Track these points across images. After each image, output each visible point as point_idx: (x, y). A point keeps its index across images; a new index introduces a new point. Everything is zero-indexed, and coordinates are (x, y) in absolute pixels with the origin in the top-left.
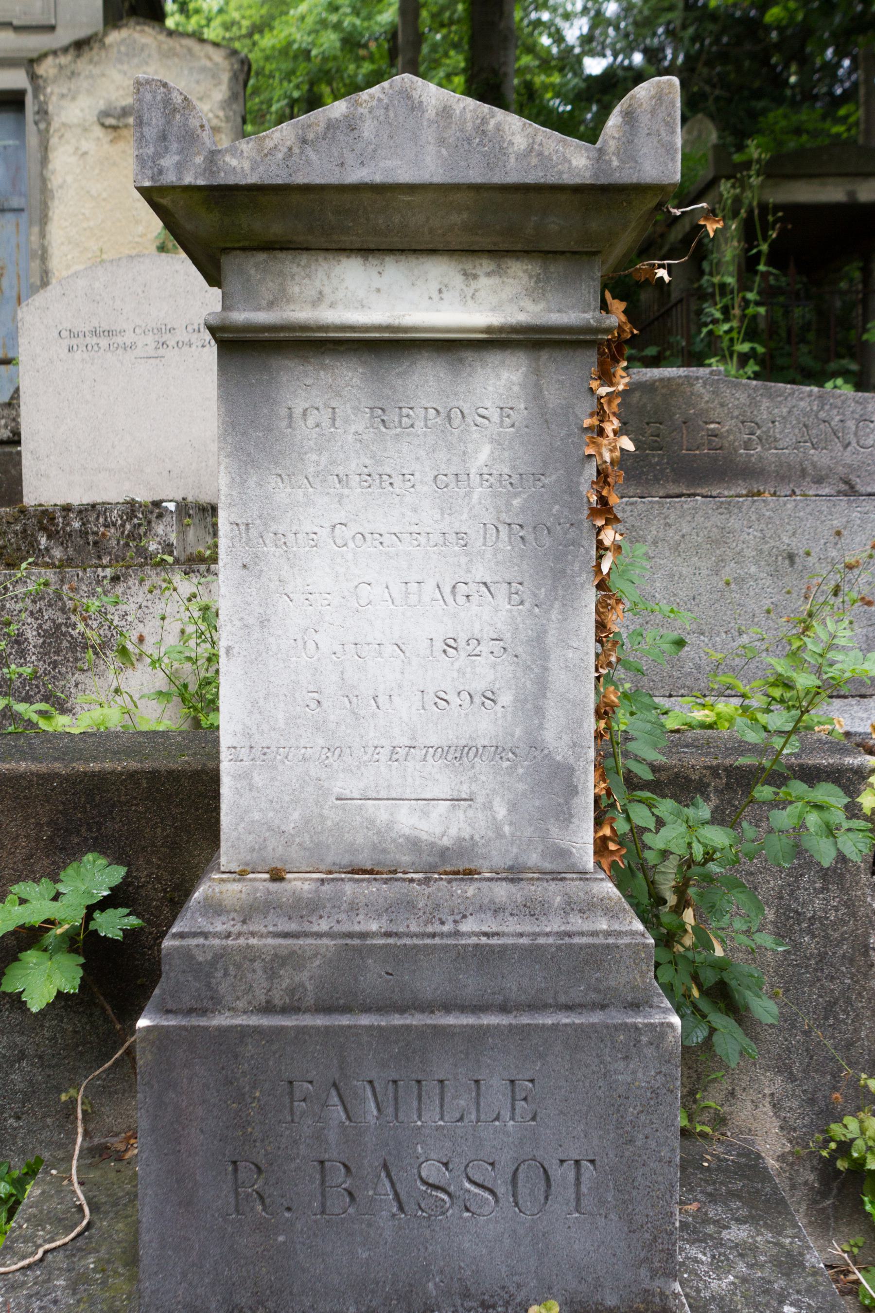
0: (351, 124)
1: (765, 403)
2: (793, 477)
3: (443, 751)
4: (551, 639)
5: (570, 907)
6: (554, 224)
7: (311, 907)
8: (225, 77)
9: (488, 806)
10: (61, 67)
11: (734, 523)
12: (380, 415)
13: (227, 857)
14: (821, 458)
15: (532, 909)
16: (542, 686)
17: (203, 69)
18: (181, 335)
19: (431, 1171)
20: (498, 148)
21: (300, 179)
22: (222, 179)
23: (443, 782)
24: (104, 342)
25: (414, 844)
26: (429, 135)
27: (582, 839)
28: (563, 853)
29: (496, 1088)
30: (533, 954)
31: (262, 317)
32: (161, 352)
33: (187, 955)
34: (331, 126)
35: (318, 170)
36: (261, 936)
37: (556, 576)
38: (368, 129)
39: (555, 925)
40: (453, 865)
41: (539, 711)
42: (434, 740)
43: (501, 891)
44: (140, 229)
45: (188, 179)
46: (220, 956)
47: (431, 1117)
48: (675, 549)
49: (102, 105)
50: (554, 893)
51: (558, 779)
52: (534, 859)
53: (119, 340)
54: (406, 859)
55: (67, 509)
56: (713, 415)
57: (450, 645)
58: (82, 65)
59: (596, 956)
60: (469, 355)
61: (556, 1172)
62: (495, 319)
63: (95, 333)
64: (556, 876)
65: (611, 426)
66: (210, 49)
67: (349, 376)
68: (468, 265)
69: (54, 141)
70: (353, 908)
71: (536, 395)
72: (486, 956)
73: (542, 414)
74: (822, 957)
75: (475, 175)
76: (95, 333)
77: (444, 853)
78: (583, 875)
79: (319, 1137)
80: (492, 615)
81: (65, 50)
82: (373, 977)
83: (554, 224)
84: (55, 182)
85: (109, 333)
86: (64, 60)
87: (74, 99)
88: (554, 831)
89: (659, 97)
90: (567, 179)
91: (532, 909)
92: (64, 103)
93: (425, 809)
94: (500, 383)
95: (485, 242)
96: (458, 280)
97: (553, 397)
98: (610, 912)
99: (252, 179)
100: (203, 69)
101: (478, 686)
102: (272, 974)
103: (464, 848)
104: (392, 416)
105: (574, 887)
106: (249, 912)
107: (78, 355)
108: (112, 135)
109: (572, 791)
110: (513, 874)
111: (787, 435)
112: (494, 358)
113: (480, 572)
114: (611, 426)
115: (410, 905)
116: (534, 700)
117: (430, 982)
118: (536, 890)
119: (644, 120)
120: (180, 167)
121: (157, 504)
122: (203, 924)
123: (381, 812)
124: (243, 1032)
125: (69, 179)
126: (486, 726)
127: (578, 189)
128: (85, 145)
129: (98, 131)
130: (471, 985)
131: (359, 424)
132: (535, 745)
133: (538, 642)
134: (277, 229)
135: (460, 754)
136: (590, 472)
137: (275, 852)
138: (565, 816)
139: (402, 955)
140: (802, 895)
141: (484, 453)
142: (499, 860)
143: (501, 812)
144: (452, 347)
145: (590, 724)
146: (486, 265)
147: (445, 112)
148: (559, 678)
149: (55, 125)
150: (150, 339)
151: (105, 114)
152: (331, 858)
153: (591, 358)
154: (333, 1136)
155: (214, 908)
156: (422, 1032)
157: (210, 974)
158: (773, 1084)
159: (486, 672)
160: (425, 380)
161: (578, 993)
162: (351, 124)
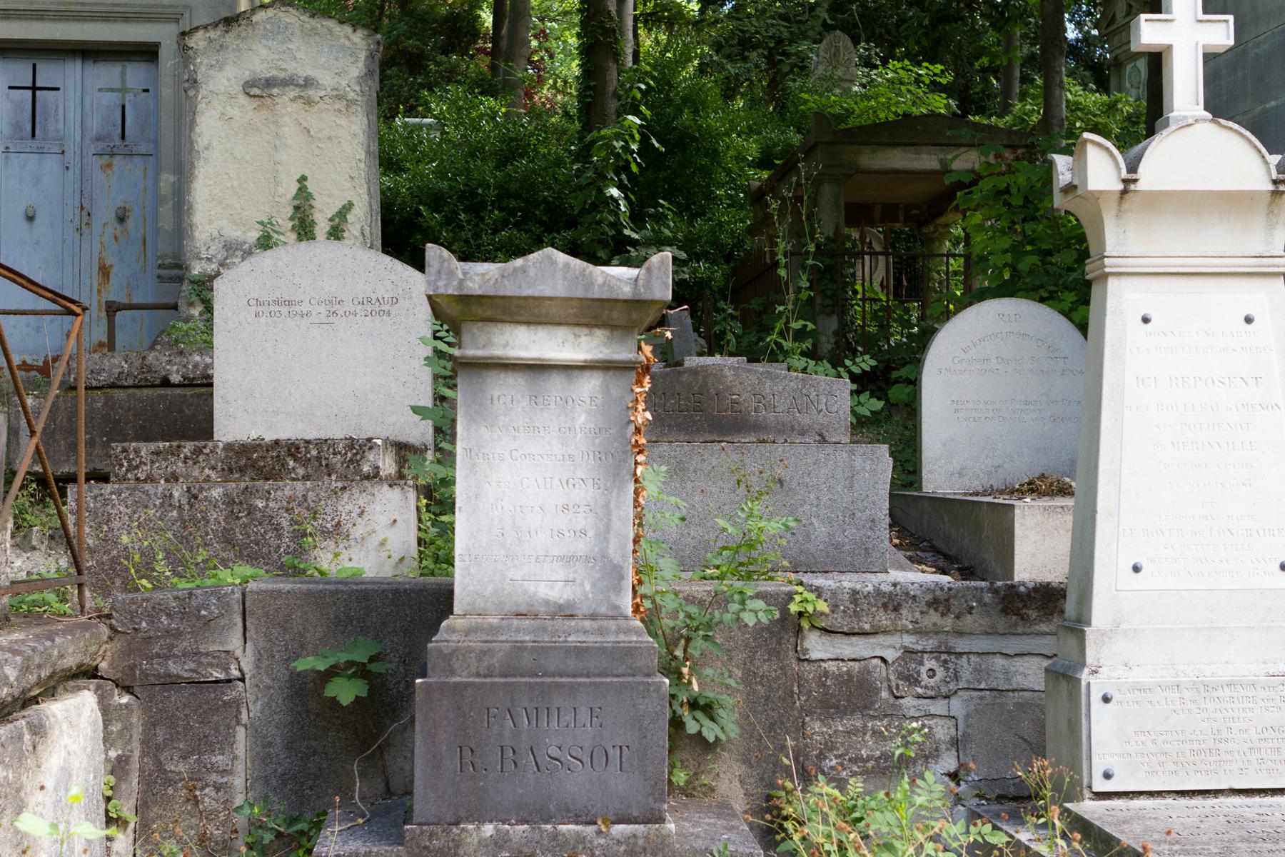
0: (524, 270)
1: (768, 383)
2: (787, 431)
3: (561, 558)
4: (612, 506)
5: (619, 630)
6: (615, 315)
8: (363, 56)
9: (582, 585)
10: (211, 40)
12: (534, 399)
13: (457, 608)
14: (804, 419)
15: (601, 631)
16: (608, 528)
17: (343, 47)
18: (348, 306)
19: (553, 751)
20: (590, 282)
21: (501, 293)
22: (465, 292)
23: (561, 574)
24: (284, 310)
25: (546, 602)
26: (559, 275)
27: (626, 602)
28: (617, 608)
29: (584, 715)
30: (602, 650)
31: (480, 353)
32: (332, 319)
33: (440, 651)
34: (515, 270)
35: (509, 290)
36: (475, 643)
38: (532, 272)
39: (612, 638)
40: (565, 612)
41: (607, 540)
42: (556, 553)
45: (450, 292)
46: (454, 651)
48: (708, 476)
49: (247, 75)
50: (612, 625)
51: (615, 573)
52: (603, 610)
53: (297, 308)
54: (542, 609)
55: (308, 442)
56: (735, 390)
57: (565, 508)
58: (230, 39)
60: (576, 373)
61: (611, 752)
62: (588, 357)
63: (277, 302)
64: (614, 618)
65: (641, 406)
68: (577, 330)
69: (201, 106)
70: (518, 630)
71: (606, 391)
72: (580, 651)
74: (767, 698)
76: (277, 302)
77: (560, 607)
78: (626, 617)
79: (500, 735)
80: (585, 493)
81: (216, 25)
82: (527, 660)
83: (615, 315)
84: (201, 143)
85: (289, 303)
86: (212, 34)
87: (221, 69)
88: (613, 597)
89: (662, 262)
90: (621, 297)
91: (601, 631)
92: (212, 73)
93: (551, 583)
94: (591, 385)
95: (584, 321)
96: (571, 337)
97: (615, 392)
98: (637, 633)
99: (479, 292)
100: (343, 47)
101: (578, 527)
102: (480, 660)
104: (540, 400)
105: (621, 622)
106: (468, 632)
107: (263, 320)
108: (256, 103)
109: (622, 577)
110: (593, 617)
111: (782, 404)
112: (587, 374)
113: (580, 474)
114: (641, 406)
115: (544, 629)
116: (604, 535)
117: (553, 664)
118: (604, 623)
119: (655, 272)
120: (447, 286)
121: (369, 440)
122: (446, 636)
123: (531, 587)
124: (467, 685)
125: (215, 142)
126: (581, 546)
127: (625, 301)
128: (230, 112)
129: (243, 99)
130: (573, 665)
131: (524, 403)
134: (488, 313)
135: (569, 560)
136: (632, 428)
137: (480, 604)
138: (618, 589)
139: (541, 650)
140: (757, 663)
141: (583, 418)
142: (587, 611)
143: (588, 587)
144: (567, 369)
145: (631, 546)
146: (585, 331)
147: (567, 265)
148: (616, 524)
149: (202, 92)
150: (322, 309)
152: (507, 609)
153: (633, 376)
154: (507, 735)
155: (452, 630)
156: (549, 685)
157: (446, 659)
158: (739, 769)
159: (582, 520)
160: (555, 383)
162: (524, 270)
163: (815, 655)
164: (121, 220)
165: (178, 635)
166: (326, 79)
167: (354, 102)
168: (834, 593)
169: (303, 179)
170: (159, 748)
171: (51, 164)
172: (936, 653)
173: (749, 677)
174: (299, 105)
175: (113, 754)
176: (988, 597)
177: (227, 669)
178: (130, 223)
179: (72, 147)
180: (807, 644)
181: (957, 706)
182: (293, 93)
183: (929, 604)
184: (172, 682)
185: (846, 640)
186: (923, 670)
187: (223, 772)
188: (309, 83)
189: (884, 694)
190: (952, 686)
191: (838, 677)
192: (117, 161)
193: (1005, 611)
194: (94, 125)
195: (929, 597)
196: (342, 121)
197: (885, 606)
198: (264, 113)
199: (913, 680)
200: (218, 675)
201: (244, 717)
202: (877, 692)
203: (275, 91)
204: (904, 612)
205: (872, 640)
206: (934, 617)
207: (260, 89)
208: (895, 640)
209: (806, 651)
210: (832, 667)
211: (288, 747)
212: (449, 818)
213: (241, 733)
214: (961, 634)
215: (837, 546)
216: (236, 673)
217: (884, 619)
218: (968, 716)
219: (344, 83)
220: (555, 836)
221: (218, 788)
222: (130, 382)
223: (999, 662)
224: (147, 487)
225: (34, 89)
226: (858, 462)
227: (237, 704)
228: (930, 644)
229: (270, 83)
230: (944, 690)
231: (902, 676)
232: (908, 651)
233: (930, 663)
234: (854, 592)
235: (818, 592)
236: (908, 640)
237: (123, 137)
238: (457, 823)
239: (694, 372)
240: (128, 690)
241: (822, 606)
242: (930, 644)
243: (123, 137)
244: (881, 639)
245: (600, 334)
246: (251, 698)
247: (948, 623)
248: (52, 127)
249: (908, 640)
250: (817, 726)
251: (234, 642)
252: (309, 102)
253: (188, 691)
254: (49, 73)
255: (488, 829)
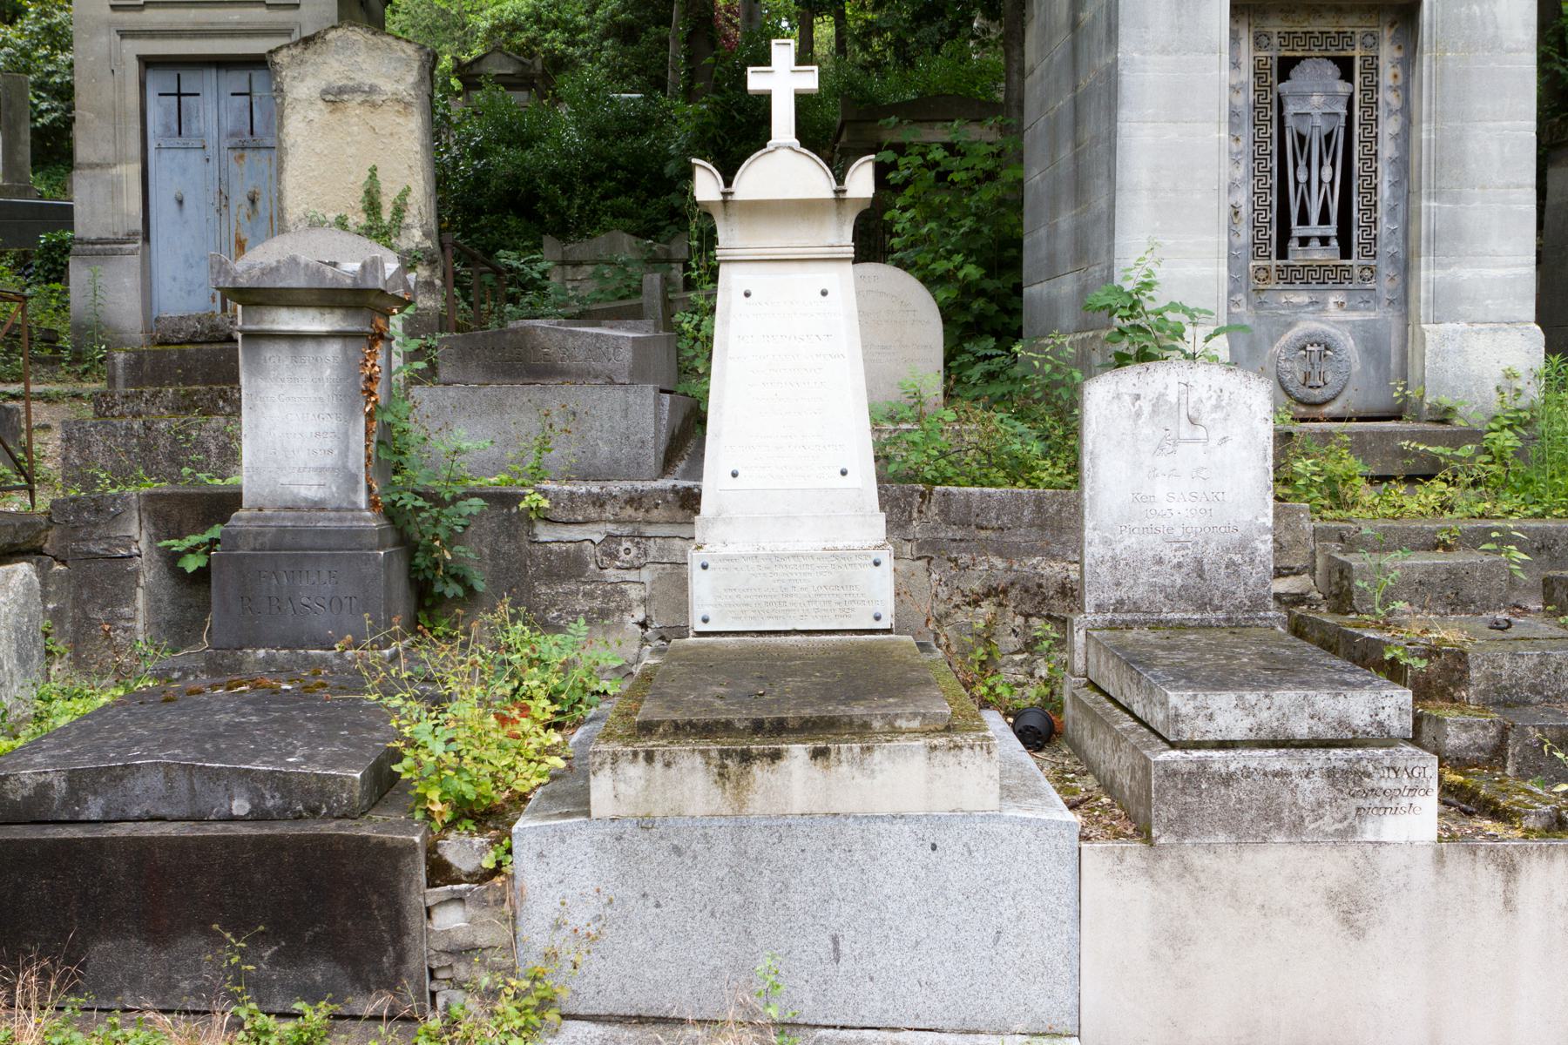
2: (581, 376)
3: (316, 469)
5: (353, 519)
7: (270, 518)
8: (416, 65)
10: (293, 57)
11: (548, 397)
12: (295, 358)
13: (244, 505)
14: (597, 366)
15: (341, 520)
16: (347, 448)
17: (399, 60)
19: (304, 600)
23: (315, 480)
25: (306, 499)
27: (362, 499)
29: (325, 575)
30: (338, 532)
31: (254, 327)
36: (253, 527)
37: (351, 412)
40: (318, 506)
42: (312, 465)
43: (332, 514)
44: (352, 178)
46: (239, 533)
47: (304, 583)
48: (520, 409)
49: (323, 85)
50: (349, 515)
51: (352, 479)
52: (345, 505)
57: (317, 434)
58: (308, 54)
59: (357, 534)
62: (337, 328)
66: (404, 45)
67: (284, 346)
69: (288, 111)
71: (345, 353)
72: (324, 533)
73: (347, 359)
75: (316, 285)
80: (331, 424)
81: (296, 44)
82: (288, 539)
84: (288, 142)
86: (294, 51)
91: (341, 520)
93: (309, 488)
94: (333, 349)
97: (351, 353)
100: (399, 60)
103: (322, 501)
105: (356, 513)
106: (249, 520)
109: (358, 482)
110: (338, 509)
113: (327, 410)
117: (306, 542)
118: (343, 514)
123: (295, 489)
124: (244, 556)
125: (299, 139)
126: (329, 461)
128: (311, 115)
129: (321, 105)
130: (319, 542)
132: (345, 467)
133: (346, 434)
134: (258, 300)
135: (320, 470)
136: (363, 378)
137: (260, 501)
138: (355, 491)
139: (297, 532)
141: (328, 372)
148: (353, 446)
151: (325, 92)
155: (239, 519)
159: (329, 443)
160: (309, 348)
161: (353, 545)
163: (542, 538)
164: (253, 201)
165: (96, 525)
166: (388, 87)
167: (408, 105)
168: (557, 494)
169: (373, 170)
170: (85, 603)
171: (195, 157)
172: (631, 537)
173: (495, 554)
174: (367, 107)
175: (50, 606)
176: (670, 497)
177: (129, 549)
178: (260, 205)
179: (211, 143)
180: (536, 531)
181: (646, 575)
182: (359, 98)
183: (626, 502)
184: (92, 557)
185: (565, 527)
186: (621, 549)
187: (129, 619)
188: (373, 89)
189: (592, 566)
190: (642, 561)
191: (558, 554)
192: (247, 153)
193: (682, 507)
194: (229, 123)
195: (626, 496)
196: (401, 120)
197: (594, 504)
198: (338, 115)
199: (614, 556)
200: (123, 552)
201: (142, 582)
202: (587, 564)
203: (345, 97)
204: (608, 507)
205: (584, 527)
206: (629, 511)
207: (334, 97)
208: (602, 527)
209: (535, 535)
210: (555, 547)
211: (172, 603)
212: (236, 645)
213: (140, 592)
214: (650, 523)
215: (617, 461)
216: (135, 551)
217: (593, 513)
218: (653, 582)
219: (401, 88)
220: (306, 657)
221: (126, 630)
222: (203, 338)
223: (677, 542)
224: (115, 421)
225: (179, 95)
226: (631, 398)
227: (136, 572)
228: (627, 530)
229: (341, 91)
230: (636, 563)
231: (605, 554)
232: (610, 536)
233: (626, 544)
234: (572, 493)
235: (545, 493)
236: (611, 528)
237: (252, 133)
238: (241, 649)
239: (515, 331)
240: (64, 563)
241: (545, 504)
242: (627, 530)
243: (252, 133)
244: (590, 526)
245: (338, 313)
246: (146, 569)
247: (641, 515)
248: (194, 127)
249: (611, 528)
250: (543, 589)
251: (134, 530)
252: (374, 105)
253: (102, 564)
254: (191, 81)
255: (261, 653)
